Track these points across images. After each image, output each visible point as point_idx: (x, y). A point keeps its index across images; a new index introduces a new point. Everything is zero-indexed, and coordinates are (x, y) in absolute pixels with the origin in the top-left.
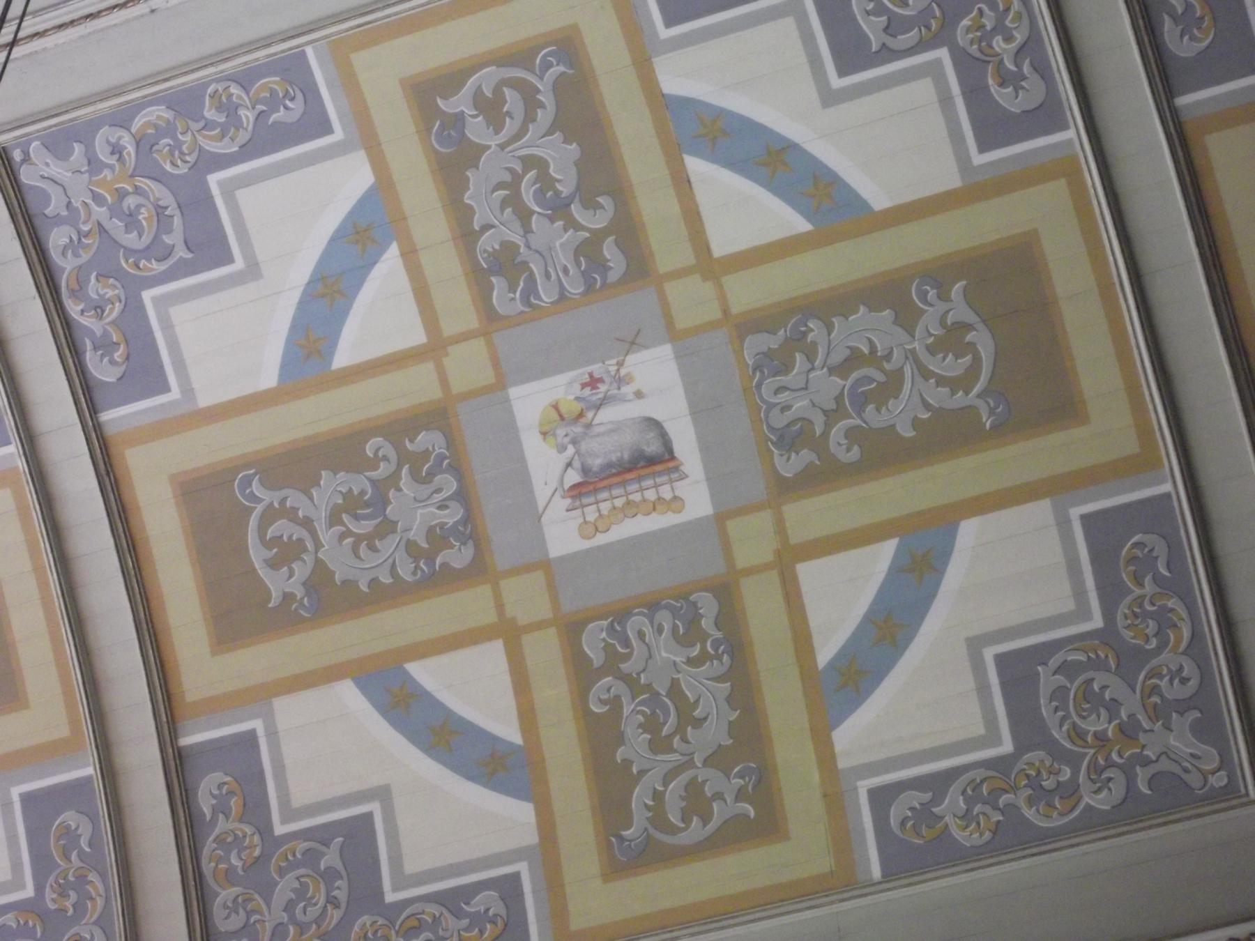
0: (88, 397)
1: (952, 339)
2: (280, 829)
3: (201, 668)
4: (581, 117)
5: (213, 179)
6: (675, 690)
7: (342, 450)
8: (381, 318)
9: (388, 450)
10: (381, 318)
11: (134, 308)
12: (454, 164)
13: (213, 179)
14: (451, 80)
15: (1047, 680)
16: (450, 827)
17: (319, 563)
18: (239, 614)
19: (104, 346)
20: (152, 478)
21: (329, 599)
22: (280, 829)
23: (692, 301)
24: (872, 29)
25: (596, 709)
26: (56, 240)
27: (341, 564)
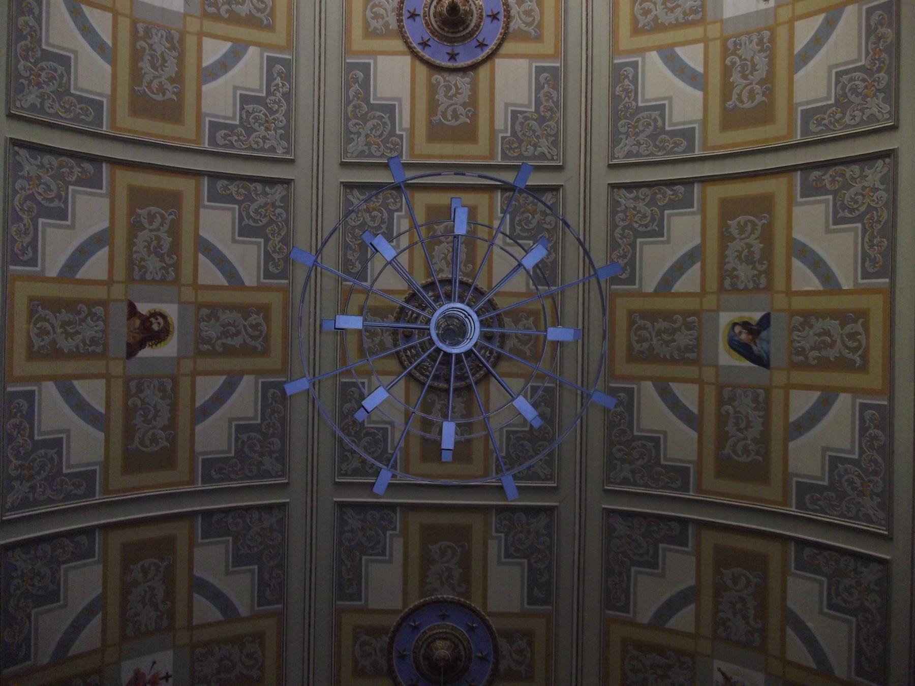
0: (214, 176)
1: (154, 440)
2: (71, 188)
3: (126, 178)
4: (246, 351)
5: (262, 240)
6: (78, 333)
7: (175, 248)
8: (210, 274)
9: (171, 262)
10: (210, 274)
11: (235, 201)
12: (244, 310)
13: (262, 240)
14: (267, 319)
15: (52, 452)
16: (57, 245)
17: (145, 228)
18: (138, 197)
19: (226, 188)
20: (185, 185)
21: (135, 228)
22: (71, 188)
23: (187, 366)
24: (244, 437)
25: (80, 305)
26: (259, 187)
27: (143, 235)
